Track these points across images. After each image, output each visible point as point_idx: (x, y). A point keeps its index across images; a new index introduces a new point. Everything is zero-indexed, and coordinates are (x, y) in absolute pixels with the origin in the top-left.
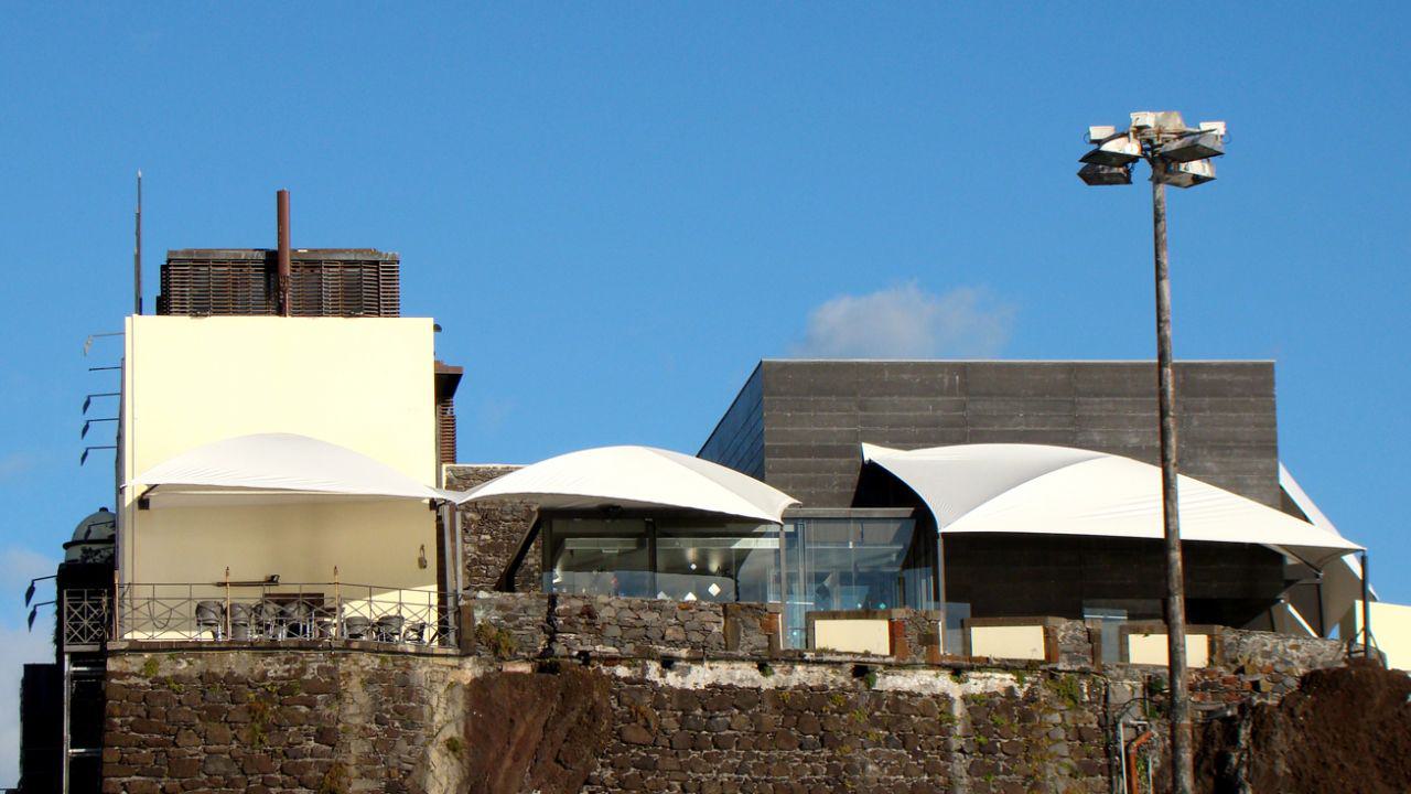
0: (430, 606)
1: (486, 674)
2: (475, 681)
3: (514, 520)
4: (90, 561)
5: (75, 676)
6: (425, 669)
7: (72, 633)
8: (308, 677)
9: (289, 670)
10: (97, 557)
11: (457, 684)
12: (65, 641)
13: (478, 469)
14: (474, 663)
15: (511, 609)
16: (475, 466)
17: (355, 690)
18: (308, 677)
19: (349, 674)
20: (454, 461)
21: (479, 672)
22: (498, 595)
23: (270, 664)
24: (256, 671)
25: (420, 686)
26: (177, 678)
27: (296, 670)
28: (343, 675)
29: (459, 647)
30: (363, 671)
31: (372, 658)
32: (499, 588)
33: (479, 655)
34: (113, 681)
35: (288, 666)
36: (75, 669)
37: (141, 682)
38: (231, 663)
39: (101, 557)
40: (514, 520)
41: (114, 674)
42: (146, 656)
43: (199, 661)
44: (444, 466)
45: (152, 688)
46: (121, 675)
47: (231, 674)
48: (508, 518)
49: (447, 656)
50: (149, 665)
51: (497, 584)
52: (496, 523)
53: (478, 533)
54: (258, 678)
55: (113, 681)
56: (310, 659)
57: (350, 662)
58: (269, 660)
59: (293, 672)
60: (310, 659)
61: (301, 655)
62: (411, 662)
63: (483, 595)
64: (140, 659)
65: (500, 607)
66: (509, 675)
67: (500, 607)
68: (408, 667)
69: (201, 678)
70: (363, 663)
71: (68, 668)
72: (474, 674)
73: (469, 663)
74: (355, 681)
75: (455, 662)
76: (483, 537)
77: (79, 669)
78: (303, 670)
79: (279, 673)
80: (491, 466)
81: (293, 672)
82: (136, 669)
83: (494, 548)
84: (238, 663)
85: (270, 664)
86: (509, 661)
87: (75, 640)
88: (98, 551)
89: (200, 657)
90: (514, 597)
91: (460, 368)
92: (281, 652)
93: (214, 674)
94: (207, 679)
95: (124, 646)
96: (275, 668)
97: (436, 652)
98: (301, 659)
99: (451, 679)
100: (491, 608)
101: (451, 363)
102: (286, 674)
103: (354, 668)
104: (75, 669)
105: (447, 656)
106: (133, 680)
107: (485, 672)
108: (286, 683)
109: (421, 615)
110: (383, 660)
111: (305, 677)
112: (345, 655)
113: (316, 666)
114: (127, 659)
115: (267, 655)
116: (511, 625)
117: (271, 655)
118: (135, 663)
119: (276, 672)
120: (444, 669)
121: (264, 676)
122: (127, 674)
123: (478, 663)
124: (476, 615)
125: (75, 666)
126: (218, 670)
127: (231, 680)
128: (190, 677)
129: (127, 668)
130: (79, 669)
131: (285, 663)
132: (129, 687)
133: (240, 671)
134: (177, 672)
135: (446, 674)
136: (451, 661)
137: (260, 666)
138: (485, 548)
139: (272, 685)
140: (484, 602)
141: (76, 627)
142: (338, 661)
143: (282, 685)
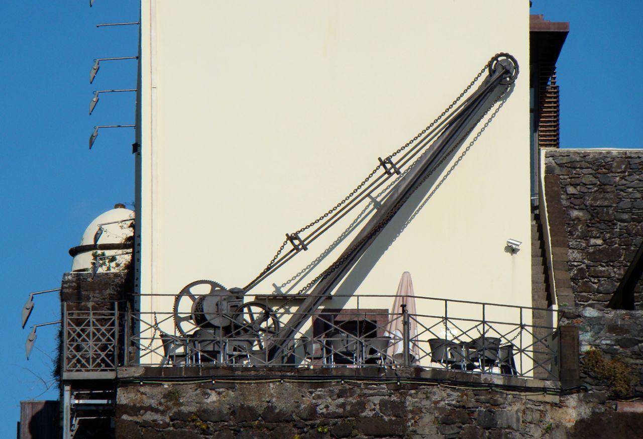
0: (522, 326)
2: (580, 423)
3: (633, 220)
4: (101, 270)
5: (76, 410)
6: (517, 406)
7: (74, 356)
8: (368, 413)
9: (343, 405)
10: (113, 264)
11: (557, 426)
12: (66, 366)
13: (585, 156)
14: (580, 400)
15: (627, 331)
16: (582, 150)
17: (427, 431)
18: (368, 413)
19: (420, 410)
20: (557, 145)
21: (585, 411)
22: (611, 314)
23: (319, 397)
24: (303, 406)
25: (509, 427)
26: (203, 414)
27: (353, 405)
28: (411, 412)
29: (560, 381)
30: (436, 408)
31: (448, 391)
32: (614, 305)
33: (586, 390)
34: (125, 417)
35: (341, 400)
36: (76, 402)
37: (158, 417)
38: (271, 395)
39: (118, 265)
40: (633, 220)
41: (125, 409)
42: (166, 386)
43: (231, 393)
44: (543, 151)
45: (174, 425)
46: (135, 410)
47: (270, 409)
48: (626, 216)
49: (544, 390)
50: (171, 396)
51: (610, 301)
52: (611, 223)
53: (585, 237)
54: (304, 415)
55: (125, 417)
56: (371, 392)
57: (420, 395)
58: (319, 391)
59: (348, 408)
60: (371, 392)
61: (359, 386)
62: (498, 397)
63: (590, 312)
64: (159, 389)
65: (613, 328)
66: (624, 415)
67: (613, 328)
68: (496, 404)
69: (233, 413)
70: (434, 398)
71: (69, 401)
72: (579, 414)
73: (572, 400)
74: (427, 418)
75: (556, 399)
76: (593, 241)
77: (81, 402)
78: (362, 406)
79: (332, 409)
80: (604, 150)
81: (348, 408)
82: (153, 403)
83: (607, 256)
84: (280, 396)
85: (319, 397)
86: (193, 413)
87: (80, 364)
88: (113, 259)
89: (232, 388)
90: (632, 316)
91: (566, 25)
92: (334, 382)
93: (250, 409)
94: (243, 416)
95: (138, 372)
96: (327, 402)
97: (529, 385)
98: (358, 391)
99: (549, 419)
100: (601, 329)
101: (552, 19)
102: (340, 410)
103: (426, 403)
104: (76, 402)
105: (544, 390)
106: (149, 416)
107: (594, 413)
108: (339, 421)
109: (509, 337)
110: (464, 393)
111: (364, 414)
112: (415, 387)
113: (377, 400)
114: (142, 389)
115: (316, 386)
116: (628, 352)
117: (322, 385)
118: (151, 395)
119: (327, 407)
120: (541, 408)
121: (313, 411)
122: (142, 408)
123: (585, 401)
124: (581, 338)
125: (78, 397)
126: (253, 404)
127: (274, 419)
128: (220, 412)
129: (142, 401)
130: (81, 402)
131: (339, 396)
132: (145, 425)
133: (281, 406)
134: (205, 406)
135: (543, 413)
136: (549, 398)
137: (308, 400)
138: (596, 256)
139: (323, 425)
140: (591, 321)
141: (78, 348)
142: (406, 394)
143: (335, 424)
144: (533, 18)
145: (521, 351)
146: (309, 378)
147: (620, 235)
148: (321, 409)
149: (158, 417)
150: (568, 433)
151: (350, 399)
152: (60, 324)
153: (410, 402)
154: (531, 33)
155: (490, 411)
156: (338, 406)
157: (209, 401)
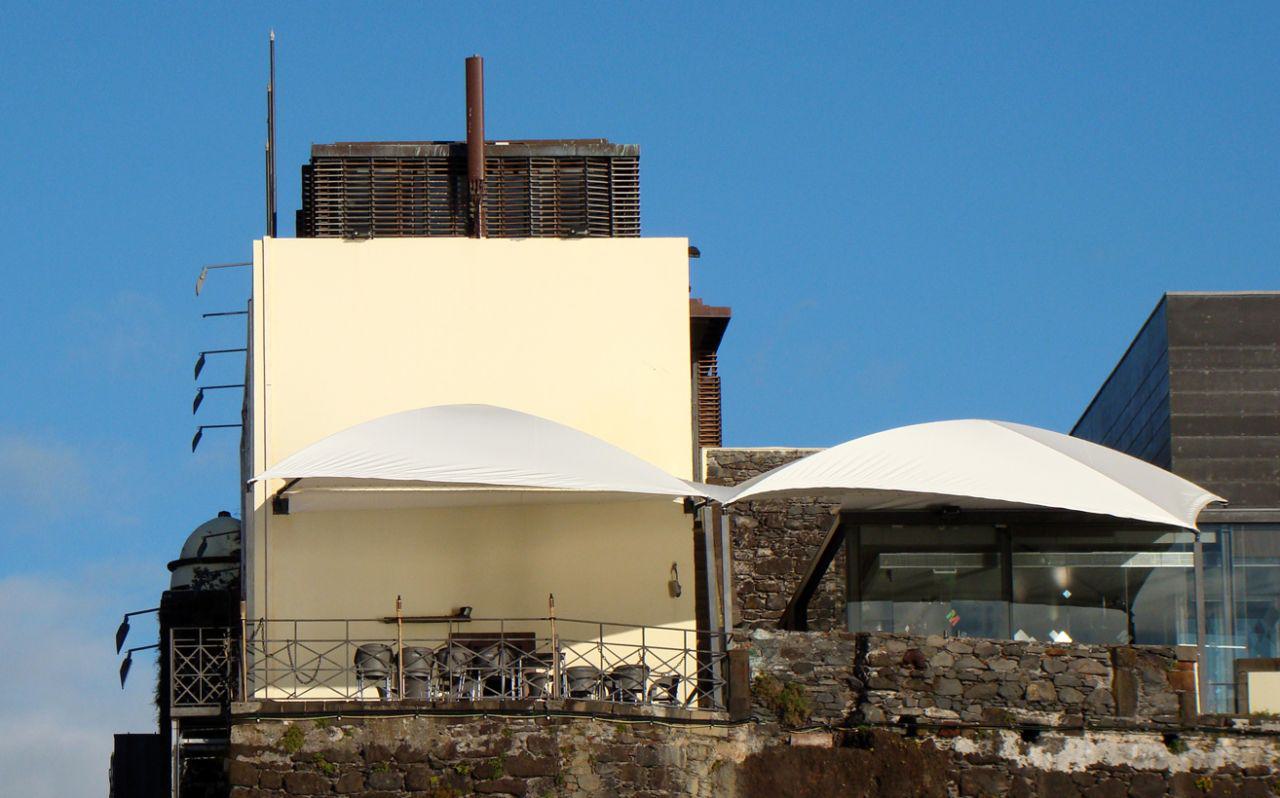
0: (686, 651)
1: (977, 754)
2: (751, 759)
3: (806, 528)
4: (205, 587)
5: (187, 751)
6: (679, 742)
7: (182, 690)
9: (486, 743)
10: (216, 582)
12: (173, 702)
13: (752, 455)
14: (750, 733)
15: (803, 655)
16: (749, 450)
17: (581, 771)
18: (514, 752)
19: (572, 748)
20: (718, 443)
21: (757, 745)
22: (783, 636)
23: (459, 734)
24: (440, 744)
25: (673, 765)
26: (329, 754)
28: (563, 749)
29: (728, 711)
32: (784, 624)
33: (757, 721)
34: (241, 758)
35: (484, 737)
36: (186, 741)
38: (405, 733)
39: (222, 581)
40: (806, 528)
41: (240, 749)
42: (286, 723)
43: (359, 730)
44: (705, 451)
45: (294, 767)
46: (251, 750)
47: (404, 748)
48: (796, 524)
49: (711, 722)
51: (781, 618)
53: (754, 545)
54: (443, 754)
55: (241, 758)
56: (518, 727)
57: (574, 731)
58: (459, 728)
59: (492, 746)
60: (518, 727)
61: (504, 720)
62: (660, 732)
63: (761, 634)
65: (787, 652)
66: (799, 748)
67: (787, 652)
68: (657, 738)
69: (362, 754)
70: (589, 733)
71: (177, 740)
73: (742, 732)
74: (581, 758)
75: (723, 731)
76: (761, 551)
77: (191, 741)
78: (507, 743)
80: (772, 449)
81: (492, 746)
82: (272, 741)
83: (776, 567)
85: (459, 734)
87: (187, 700)
88: (217, 574)
89: (361, 724)
90: (807, 639)
91: (727, 310)
92: (475, 717)
93: (381, 748)
94: (371, 754)
95: (256, 708)
96: (467, 740)
97: (695, 716)
99: (716, 755)
100: (773, 653)
101: (714, 302)
102: (483, 749)
103: (579, 739)
104: (186, 741)
105: (711, 722)
106: (267, 757)
107: (765, 747)
109: (673, 664)
110: (620, 726)
111: (509, 753)
112: (566, 721)
113: (524, 736)
114: (259, 727)
115: (455, 722)
116: (803, 678)
118: (270, 733)
119: (468, 745)
120: (707, 742)
122: (259, 748)
123: (756, 732)
124: (752, 664)
125: (186, 736)
128: (347, 751)
129: (259, 740)
130: (191, 741)
131: (482, 732)
132: (262, 766)
133: (417, 743)
135: (709, 749)
136: (717, 731)
137: (446, 737)
138: (764, 568)
139: (464, 764)
140: (764, 645)
141: (187, 681)
144: (692, 301)
145: (686, 679)
146: (446, 712)
147: (791, 545)
148: (461, 748)
149: (276, 758)
150: (737, 769)
151: (494, 736)
152: (155, 654)
153: (561, 739)
154: (692, 319)
155: (651, 747)
156: (480, 745)
157: (335, 739)
